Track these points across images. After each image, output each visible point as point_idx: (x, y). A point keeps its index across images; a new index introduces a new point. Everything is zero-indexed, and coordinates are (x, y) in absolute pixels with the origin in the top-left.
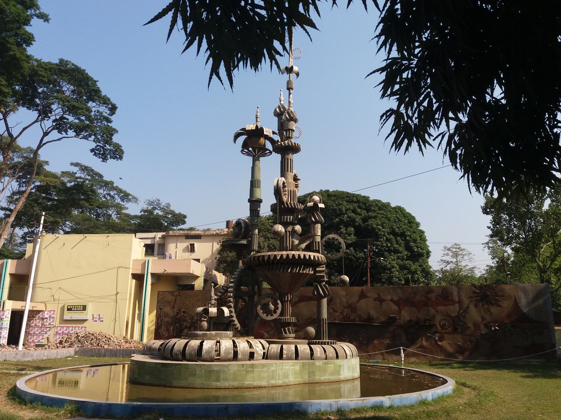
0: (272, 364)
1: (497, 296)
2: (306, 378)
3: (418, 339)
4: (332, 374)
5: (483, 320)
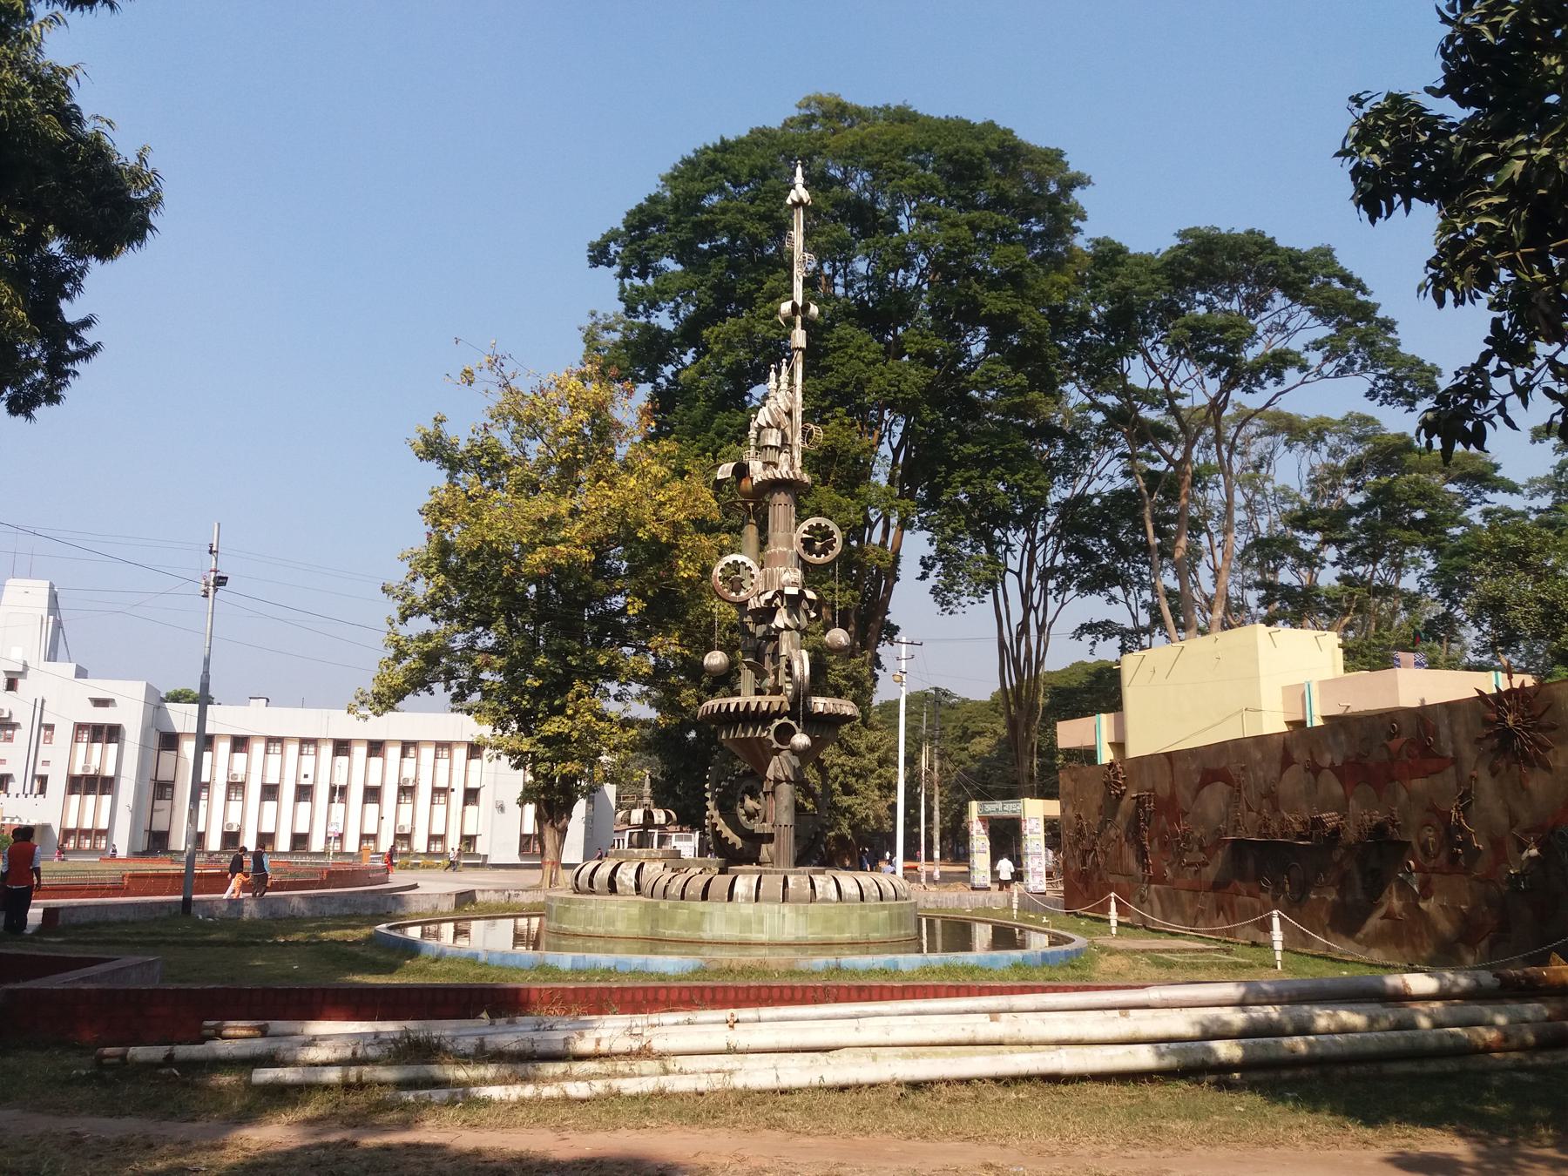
0: (591, 901)
1: (1541, 729)
2: (647, 930)
3: (1381, 892)
4: (685, 927)
5: (1512, 827)
